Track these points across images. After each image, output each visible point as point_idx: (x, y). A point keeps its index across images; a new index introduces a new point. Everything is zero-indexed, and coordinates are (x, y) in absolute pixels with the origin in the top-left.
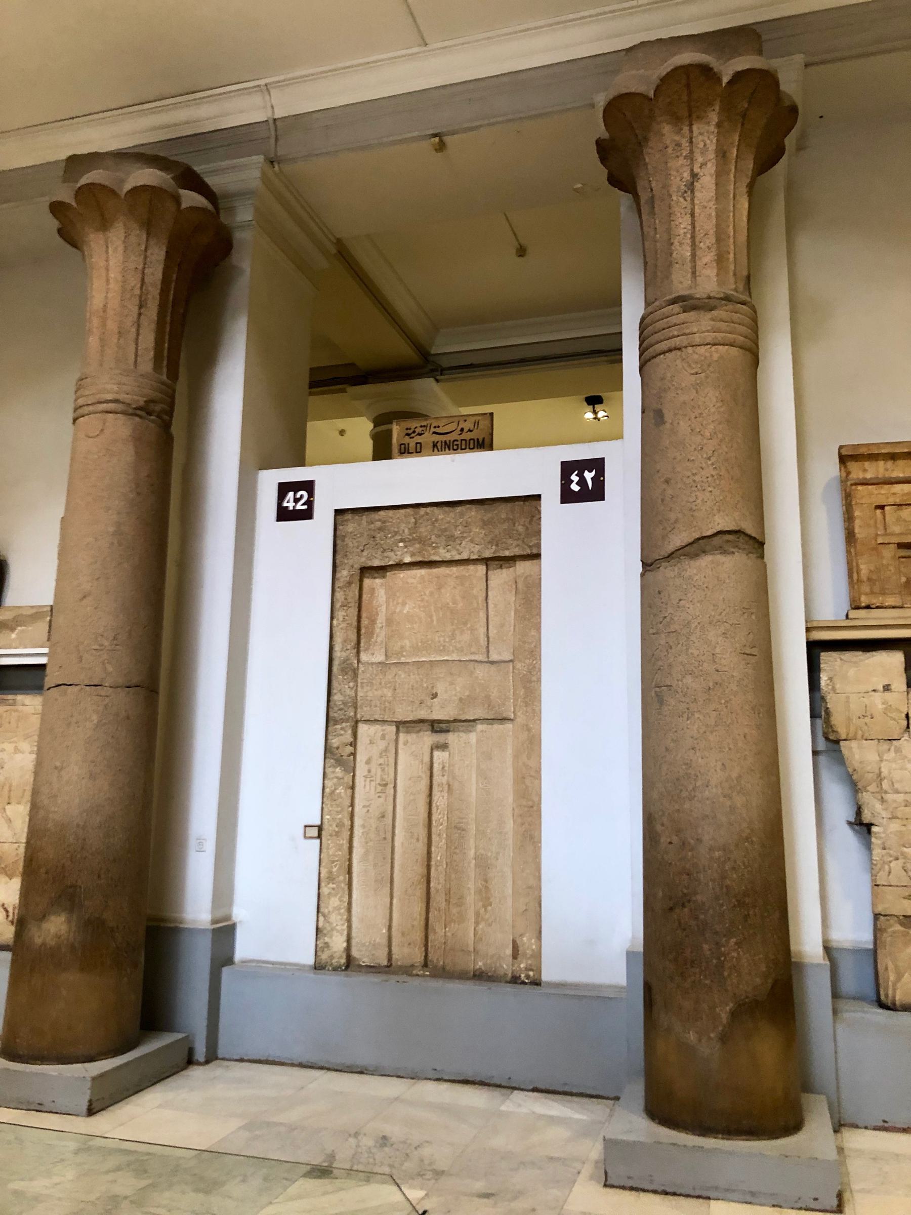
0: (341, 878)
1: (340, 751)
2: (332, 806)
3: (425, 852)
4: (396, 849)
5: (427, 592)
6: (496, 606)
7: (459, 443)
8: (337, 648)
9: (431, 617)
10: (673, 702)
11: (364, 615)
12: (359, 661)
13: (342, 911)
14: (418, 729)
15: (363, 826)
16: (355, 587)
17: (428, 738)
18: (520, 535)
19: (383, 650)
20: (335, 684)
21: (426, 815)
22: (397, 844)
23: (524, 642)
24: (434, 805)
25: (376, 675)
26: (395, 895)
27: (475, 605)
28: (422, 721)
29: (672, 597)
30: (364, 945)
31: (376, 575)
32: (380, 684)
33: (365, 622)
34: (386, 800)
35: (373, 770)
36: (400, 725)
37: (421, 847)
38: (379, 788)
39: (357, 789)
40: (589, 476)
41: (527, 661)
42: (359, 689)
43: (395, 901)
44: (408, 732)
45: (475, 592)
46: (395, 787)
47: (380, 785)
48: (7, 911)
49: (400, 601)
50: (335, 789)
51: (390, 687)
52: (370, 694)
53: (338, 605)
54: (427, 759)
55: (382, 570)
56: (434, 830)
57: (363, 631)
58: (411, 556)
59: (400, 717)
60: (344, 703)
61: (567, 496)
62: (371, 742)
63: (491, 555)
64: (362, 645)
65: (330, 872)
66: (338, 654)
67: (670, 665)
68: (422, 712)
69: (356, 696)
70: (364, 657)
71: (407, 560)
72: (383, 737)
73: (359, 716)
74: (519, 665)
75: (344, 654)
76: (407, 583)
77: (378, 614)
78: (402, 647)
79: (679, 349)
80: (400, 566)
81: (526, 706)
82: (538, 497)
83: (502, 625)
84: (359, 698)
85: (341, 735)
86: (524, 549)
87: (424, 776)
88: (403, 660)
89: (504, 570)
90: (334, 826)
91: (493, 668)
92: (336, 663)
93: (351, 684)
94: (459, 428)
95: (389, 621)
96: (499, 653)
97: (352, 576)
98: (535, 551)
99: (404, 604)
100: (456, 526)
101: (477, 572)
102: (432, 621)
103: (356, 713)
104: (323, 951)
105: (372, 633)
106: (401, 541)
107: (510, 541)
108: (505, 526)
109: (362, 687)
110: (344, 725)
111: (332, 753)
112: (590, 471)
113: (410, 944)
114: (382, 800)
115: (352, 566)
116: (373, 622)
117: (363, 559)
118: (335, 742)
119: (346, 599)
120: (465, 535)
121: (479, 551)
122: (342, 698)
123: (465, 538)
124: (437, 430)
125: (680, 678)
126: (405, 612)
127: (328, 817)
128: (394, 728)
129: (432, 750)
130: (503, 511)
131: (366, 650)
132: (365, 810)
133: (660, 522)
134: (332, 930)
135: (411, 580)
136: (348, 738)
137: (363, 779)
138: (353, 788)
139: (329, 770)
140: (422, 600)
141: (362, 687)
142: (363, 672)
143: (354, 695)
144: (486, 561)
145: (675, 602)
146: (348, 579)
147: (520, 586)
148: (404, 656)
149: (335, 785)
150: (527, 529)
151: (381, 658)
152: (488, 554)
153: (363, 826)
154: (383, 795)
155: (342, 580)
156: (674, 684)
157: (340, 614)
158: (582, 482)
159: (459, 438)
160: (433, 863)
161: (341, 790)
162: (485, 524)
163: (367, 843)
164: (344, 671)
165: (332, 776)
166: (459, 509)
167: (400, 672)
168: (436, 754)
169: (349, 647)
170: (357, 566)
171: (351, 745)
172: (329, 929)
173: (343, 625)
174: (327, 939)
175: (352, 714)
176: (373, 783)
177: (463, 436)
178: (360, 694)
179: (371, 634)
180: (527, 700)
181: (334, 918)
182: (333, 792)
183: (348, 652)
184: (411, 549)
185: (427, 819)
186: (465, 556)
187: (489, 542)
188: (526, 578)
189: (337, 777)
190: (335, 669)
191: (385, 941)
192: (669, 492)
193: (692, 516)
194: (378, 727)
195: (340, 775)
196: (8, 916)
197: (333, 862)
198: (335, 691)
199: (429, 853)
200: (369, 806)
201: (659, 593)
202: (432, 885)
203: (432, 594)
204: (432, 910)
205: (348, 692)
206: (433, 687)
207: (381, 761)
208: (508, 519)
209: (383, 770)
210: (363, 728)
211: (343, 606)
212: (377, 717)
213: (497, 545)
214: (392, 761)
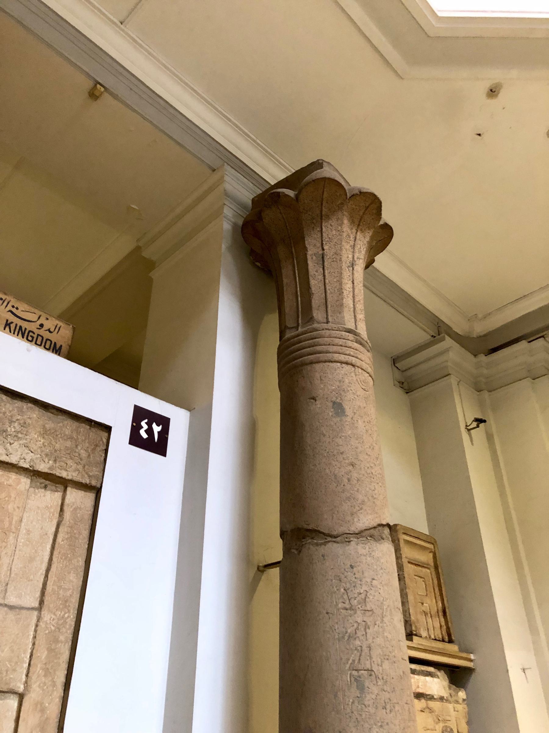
6: (28, 532)
7: (35, 336)
10: (375, 690)
18: (81, 459)
23: (60, 587)
27: (7, 524)
29: (366, 574)
40: (157, 429)
41: (58, 613)
45: (10, 507)
61: (135, 440)
63: (46, 470)
67: (370, 647)
74: (47, 616)
79: (353, 366)
81: (45, 676)
82: (108, 429)
83: (31, 559)
86: (83, 477)
89: (48, 493)
91: (11, 615)
94: (39, 322)
96: (19, 596)
98: (94, 483)
100: (11, 422)
101: (19, 483)
107: (70, 462)
108: (69, 444)
112: (158, 425)
120: (20, 435)
121: (32, 460)
123: (19, 439)
124: (14, 310)
125: (380, 663)
130: (69, 426)
133: (348, 498)
144: (34, 474)
145: (369, 580)
147: (67, 515)
150: (89, 455)
152: (43, 467)
156: (375, 668)
158: (150, 431)
159: (37, 332)
162: (45, 433)
166: (18, 403)
177: (42, 332)
180: (49, 666)
186: (13, 459)
187: (47, 455)
188: (75, 509)
192: (355, 475)
193: (374, 502)
201: (352, 567)
208: (71, 438)
213: (55, 461)
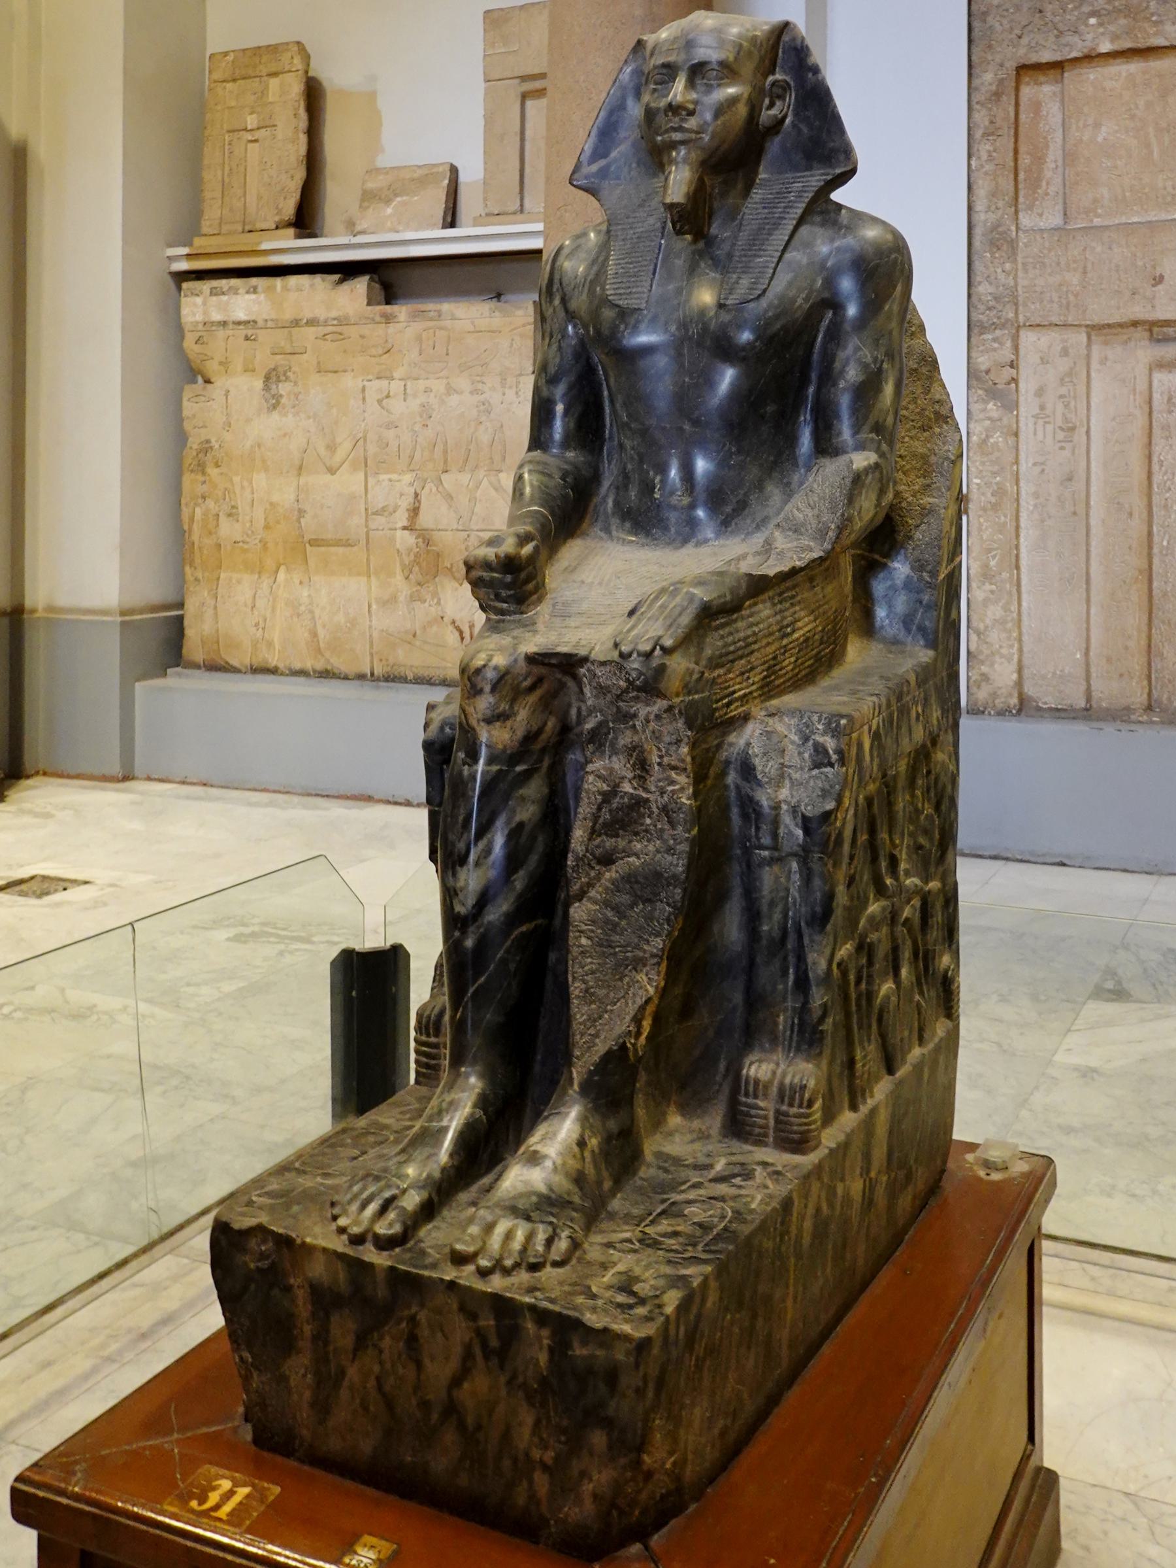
0: (1005, 575)
1: (992, 376)
2: (983, 463)
3: (1145, 533)
4: (1093, 531)
5: (1141, 103)
8: (979, 206)
9: (1148, 146)
11: (1023, 149)
12: (1018, 229)
13: (1010, 625)
14: (1125, 337)
15: (1036, 495)
16: (1008, 101)
17: (1144, 352)
19: (1060, 207)
20: (978, 266)
21: (1144, 476)
22: (1093, 522)
24: (1155, 459)
25: (1050, 250)
26: (1093, 599)
28: (1135, 324)
30: (1044, 677)
31: (1042, 79)
32: (1058, 264)
33: (1025, 160)
34: (1073, 453)
35: (1049, 406)
36: (1096, 329)
37: (1137, 525)
38: (1061, 435)
39: (1022, 436)
42: (1020, 274)
43: (1093, 611)
44: (1106, 343)
46: (1088, 432)
47: (1061, 428)
48: (461, 633)
49: (1090, 121)
50: (987, 437)
51: (1075, 270)
52: (1040, 282)
53: (978, 134)
54: (1142, 386)
55: (1058, 66)
56: (1156, 499)
57: (1022, 176)
58: (1112, 41)
59: (1096, 320)
60: (995, 298)
62: (1043, 361)
64: (1021, 200)
65: (986, 566)
66: (980, 217)
68: (1137, 309)
69: (1016, 285)
70: (1025, 220)
71: (1105, 47)
72: (1065, 352)
73: (1021, 319)
75: (992, 217)
76: (1104, 90)
77: (1047, 146)
78: (1095, 201)
80: (1090, 58)
84: (1019, 289)
85: (995, 350)
87: (1138, 412)
88: (1097, 221)
90: (989, 495)
92: (978, 231)
93: (1008, 266)
95: (1069, 157)
97: (1001, 81)
99: (1097, 125)
102: (1151, 153)
103: (1016, 313)
104: (979, 687)
105: (1039, 179)
106: (1093, 14)
109: (1026, 271)
110: (998, 332)
111: (978, 379)
113: (1121, 675)
114: (1067, 453)
115: (1001, 65)
116: (1039, 160)
117: (1022, 51)
118: (983, 362)
119: (992, 122)
122: (991, 289)
126: (1100, 139)
127: (978, 481)
128: (1083, 338)
129: (1151, 370)
131: (1030, 208)
132: (1038, 469)
134: (993, 654)
135: (1109, 84)
136: (1006, 354)
137: (1032, 420)
138: (1016, 435)
139: (976, 407)
140: (1133, 117)
141: (1026, 271)
142: (1026, 245)
143: (1012, 283)
146: (994, 88)
148: (1098, 216)
149: (987, 430)
151: (1056, 220)
153: (1036, 495)
154: (1068, 446)
155: (983, 90)
157: (984, 148)
160: (1156, 550)
161: (997, 438)
163: (1043, 521)
164: (994, 245)
165: (981, 416)
167: (1094, 244)
168: (1158, 376)
169: (1001, 204)
170: (1011, 65)
171: (1012, 366)
172: (986, 652)
173: (988, 167)
174: (984, 669)
175: (1011, 315)
176: (1050, 428)
178: (1022, 282)
179: (1035, 183)
181: (994, 636)
182: (984, 441)
183: (1000, 212)
184: (1112, 28)
185: (1146, 483)
189: (989, 418)
190: (977, 243)
191: (1080, 672)
194: (1054, 335)
195: (995, 415)
196: (462, 639)
197: (989, 550)
198: (978, 279)
199: (1150, 534)
200: (1042, 464)
202: (1155, 584)
203: (1149, 105)
204: (1155, 622)
205: (1001, 276)
206: (1154, 267)
207: (1063, 391)
209: (1067, 406)
210: (1028, 338)
211: (986, 134)
212: (1055, 319)
214: (1081, 388)
